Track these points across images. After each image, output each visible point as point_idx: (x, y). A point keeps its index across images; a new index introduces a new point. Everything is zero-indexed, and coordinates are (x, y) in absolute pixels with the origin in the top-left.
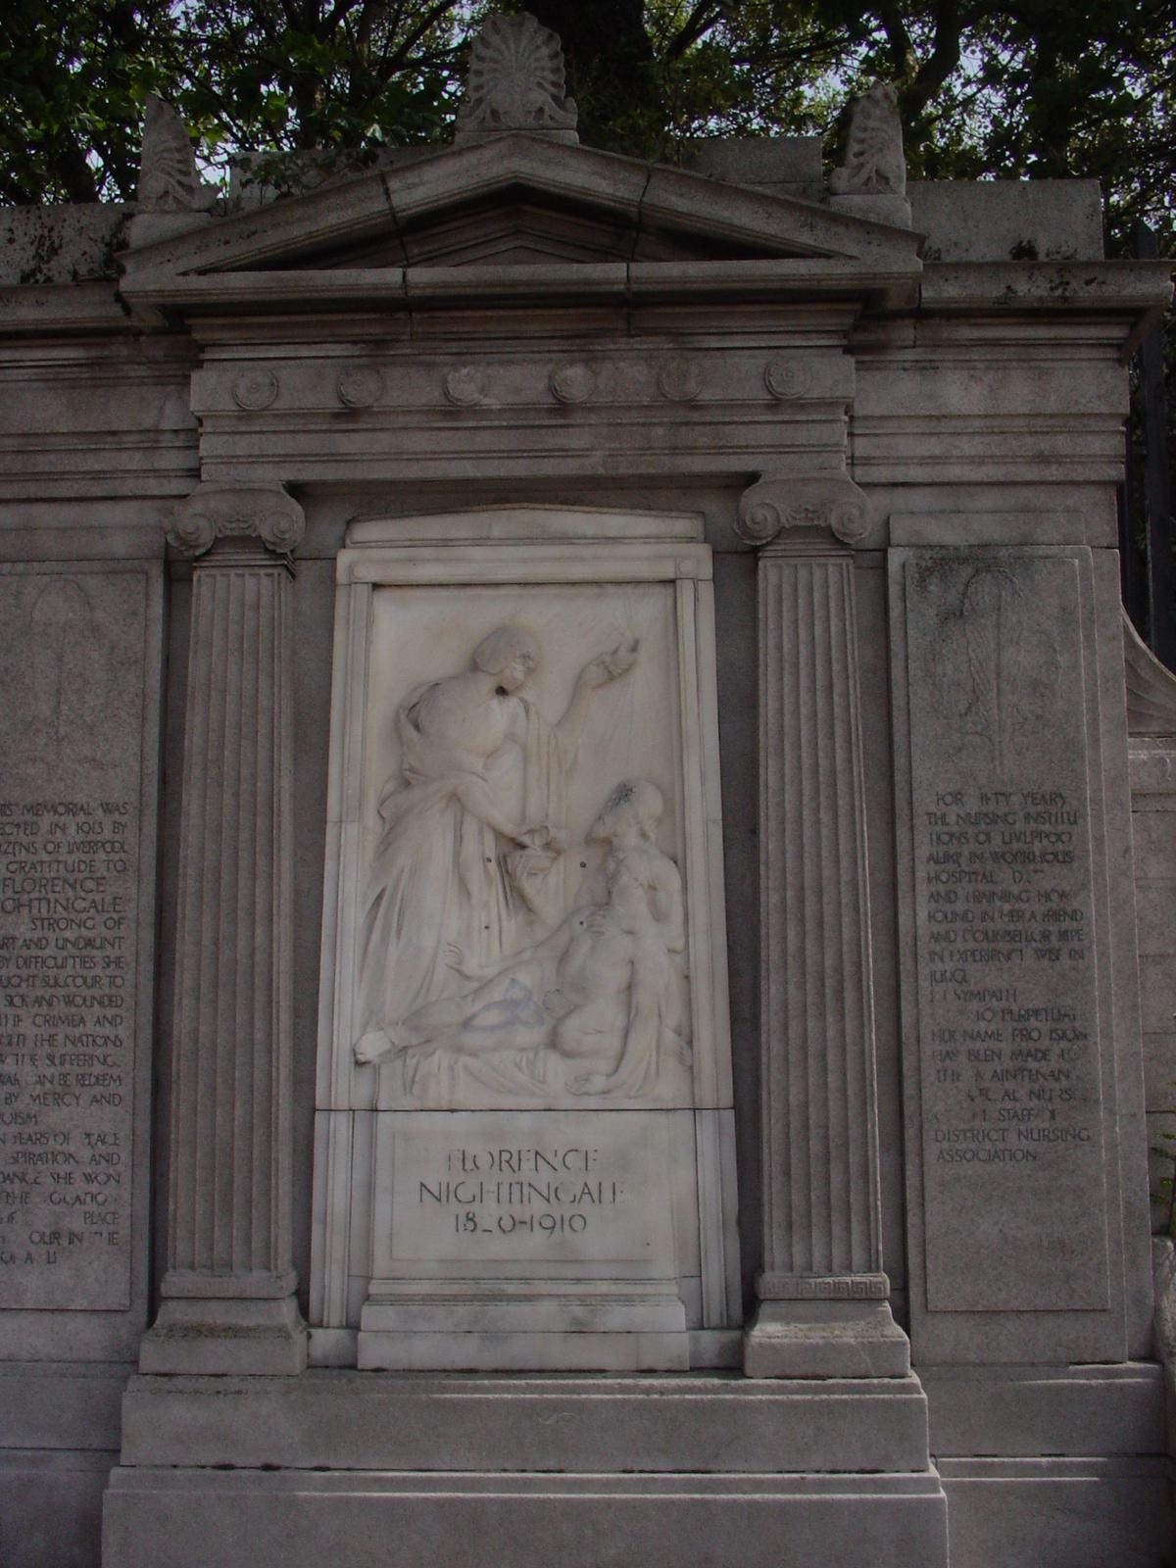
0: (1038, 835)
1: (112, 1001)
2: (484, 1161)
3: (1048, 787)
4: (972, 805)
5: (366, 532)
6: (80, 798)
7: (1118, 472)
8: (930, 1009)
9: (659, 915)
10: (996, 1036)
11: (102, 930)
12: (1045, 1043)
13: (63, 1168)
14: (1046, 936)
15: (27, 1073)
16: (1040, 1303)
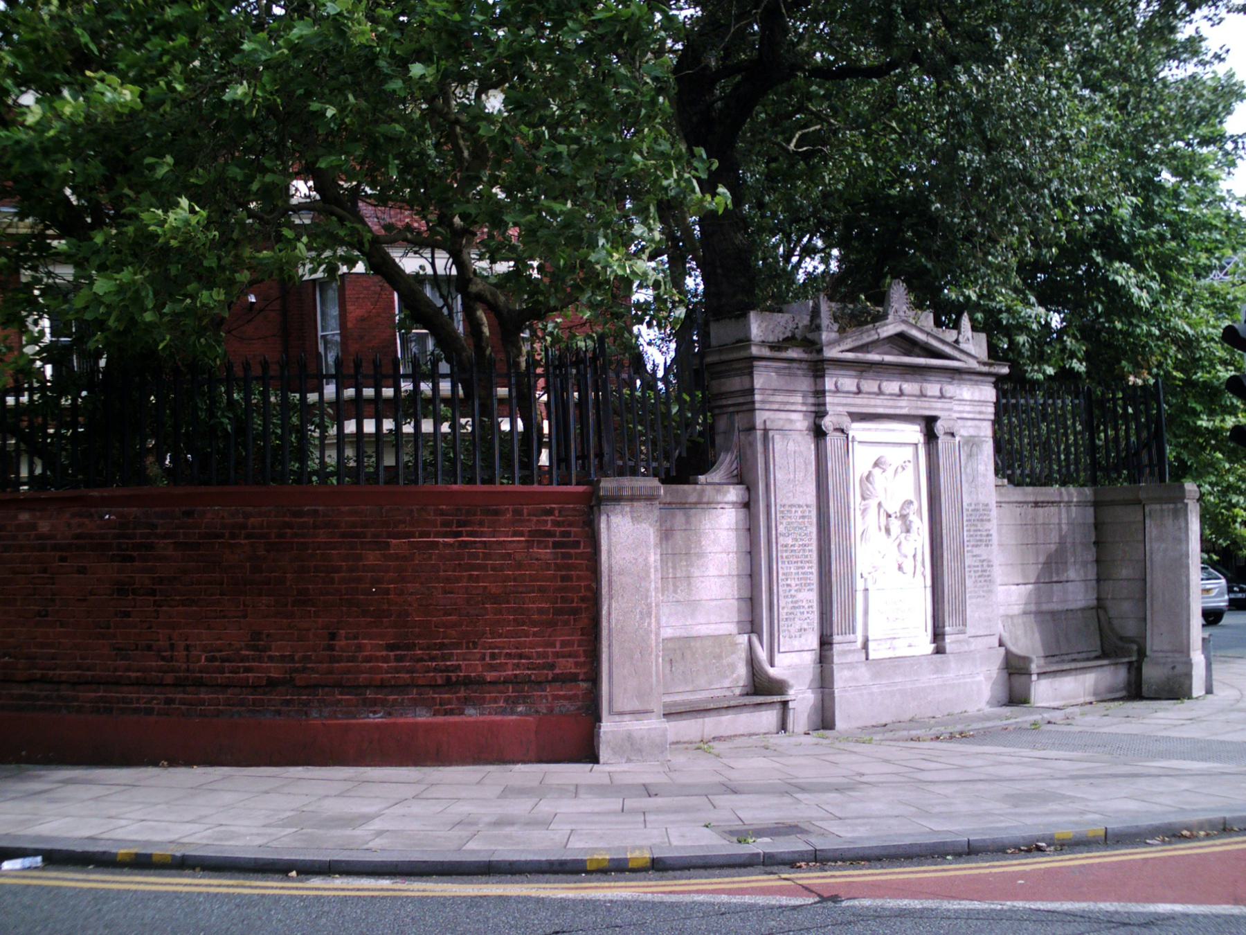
7: (992, 417)
15: (793, 583)
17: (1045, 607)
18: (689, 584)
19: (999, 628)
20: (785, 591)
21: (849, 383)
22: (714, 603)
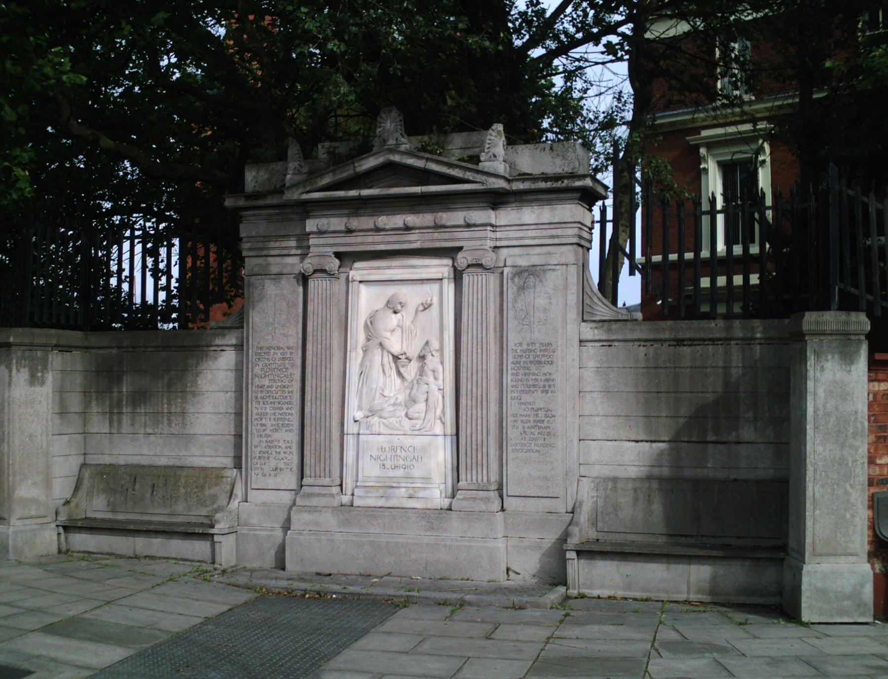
0: (543, 356)
1: (290, 403)
2: (387, 449)
3: (547, 341)
4: (525, 347)
5: (358, 265)
6: (281, 345)
8: (512, 408)
9: (436, 378)
10: (529, 416)
11: (287, 383)
12: (543, 418)
13: (278, 450)
14: (544, 386)
15: (268, 423)
16: (540, 495)
17: (688, 473)
18: (184, 419)
19: (587, 494)
20: (258, 431)
21: (337, 223)
22: (207, 438)
